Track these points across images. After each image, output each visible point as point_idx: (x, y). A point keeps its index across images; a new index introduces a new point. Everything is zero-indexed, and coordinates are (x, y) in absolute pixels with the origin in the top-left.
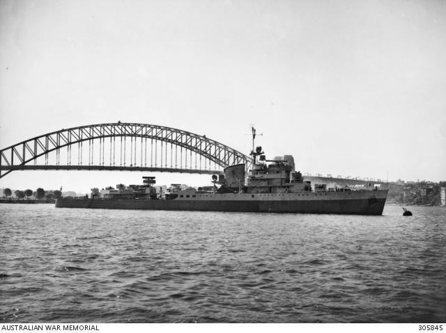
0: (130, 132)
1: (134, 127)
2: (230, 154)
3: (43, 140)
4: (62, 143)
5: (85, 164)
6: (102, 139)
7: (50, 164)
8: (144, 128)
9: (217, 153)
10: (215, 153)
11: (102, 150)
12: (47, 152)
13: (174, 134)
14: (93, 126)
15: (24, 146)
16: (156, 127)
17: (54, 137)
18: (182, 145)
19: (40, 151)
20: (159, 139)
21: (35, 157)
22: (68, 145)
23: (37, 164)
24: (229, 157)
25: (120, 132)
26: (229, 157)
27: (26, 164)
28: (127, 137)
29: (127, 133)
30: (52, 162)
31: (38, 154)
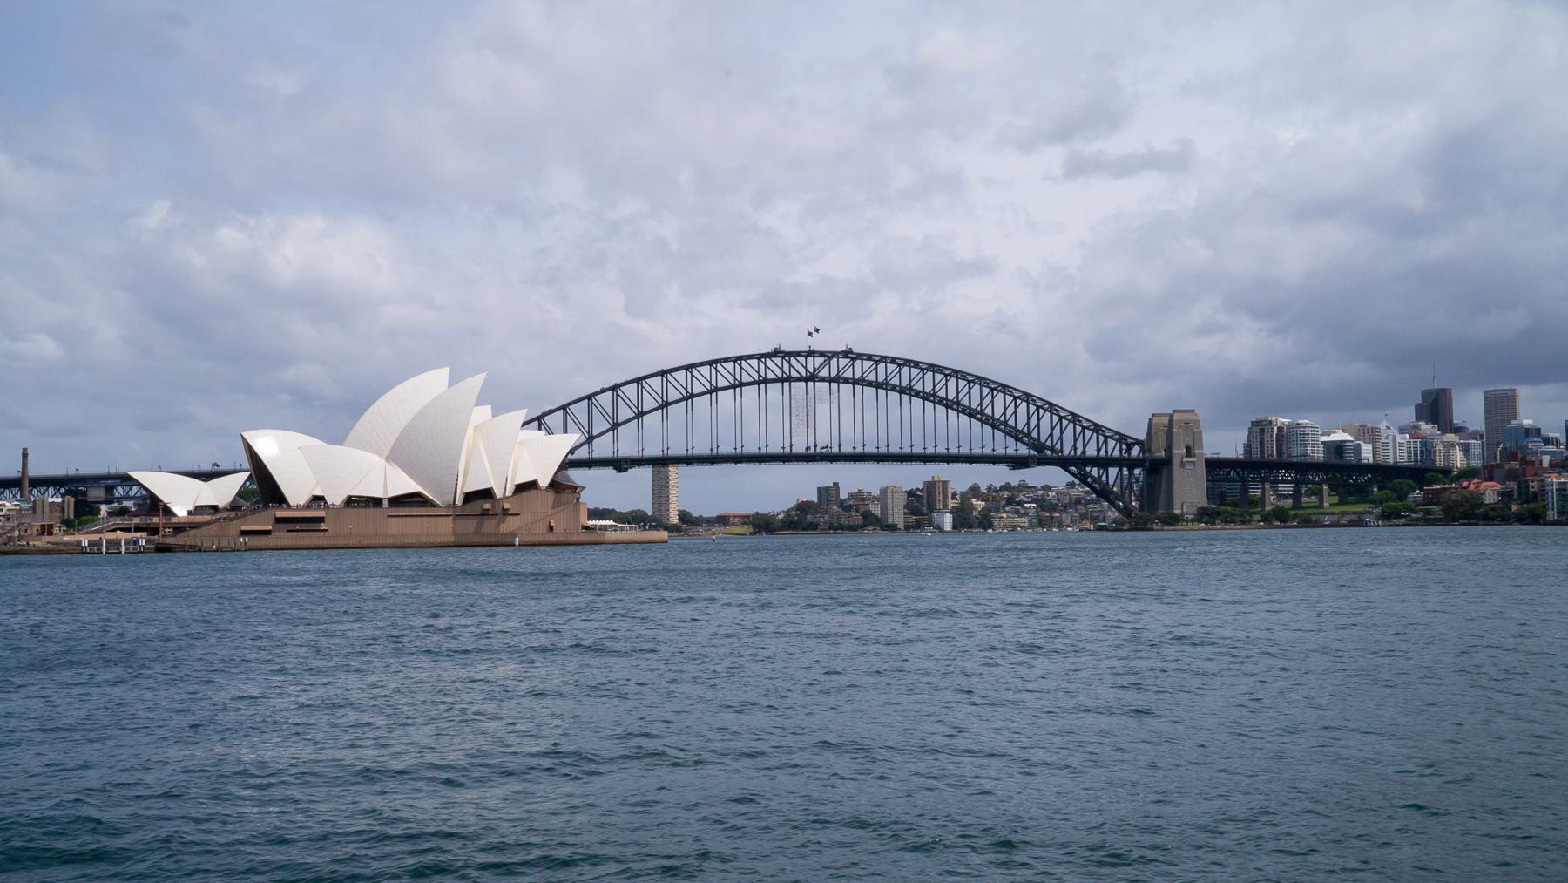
0: (803, 373)
1: (810, 359)
4: (649, 403)
5: (702, 449)
8: (835, 360)
9: (1033, 421)
10: (1028, 424)
12: (615, 426)
14: (741, 358)
15: (565, 414)
20: (894, 388)
22: (661, 407)
23: (597, 455)
25: (779, 374)
29: (794, 374)
30: (627, 450)
31: (595, 433)
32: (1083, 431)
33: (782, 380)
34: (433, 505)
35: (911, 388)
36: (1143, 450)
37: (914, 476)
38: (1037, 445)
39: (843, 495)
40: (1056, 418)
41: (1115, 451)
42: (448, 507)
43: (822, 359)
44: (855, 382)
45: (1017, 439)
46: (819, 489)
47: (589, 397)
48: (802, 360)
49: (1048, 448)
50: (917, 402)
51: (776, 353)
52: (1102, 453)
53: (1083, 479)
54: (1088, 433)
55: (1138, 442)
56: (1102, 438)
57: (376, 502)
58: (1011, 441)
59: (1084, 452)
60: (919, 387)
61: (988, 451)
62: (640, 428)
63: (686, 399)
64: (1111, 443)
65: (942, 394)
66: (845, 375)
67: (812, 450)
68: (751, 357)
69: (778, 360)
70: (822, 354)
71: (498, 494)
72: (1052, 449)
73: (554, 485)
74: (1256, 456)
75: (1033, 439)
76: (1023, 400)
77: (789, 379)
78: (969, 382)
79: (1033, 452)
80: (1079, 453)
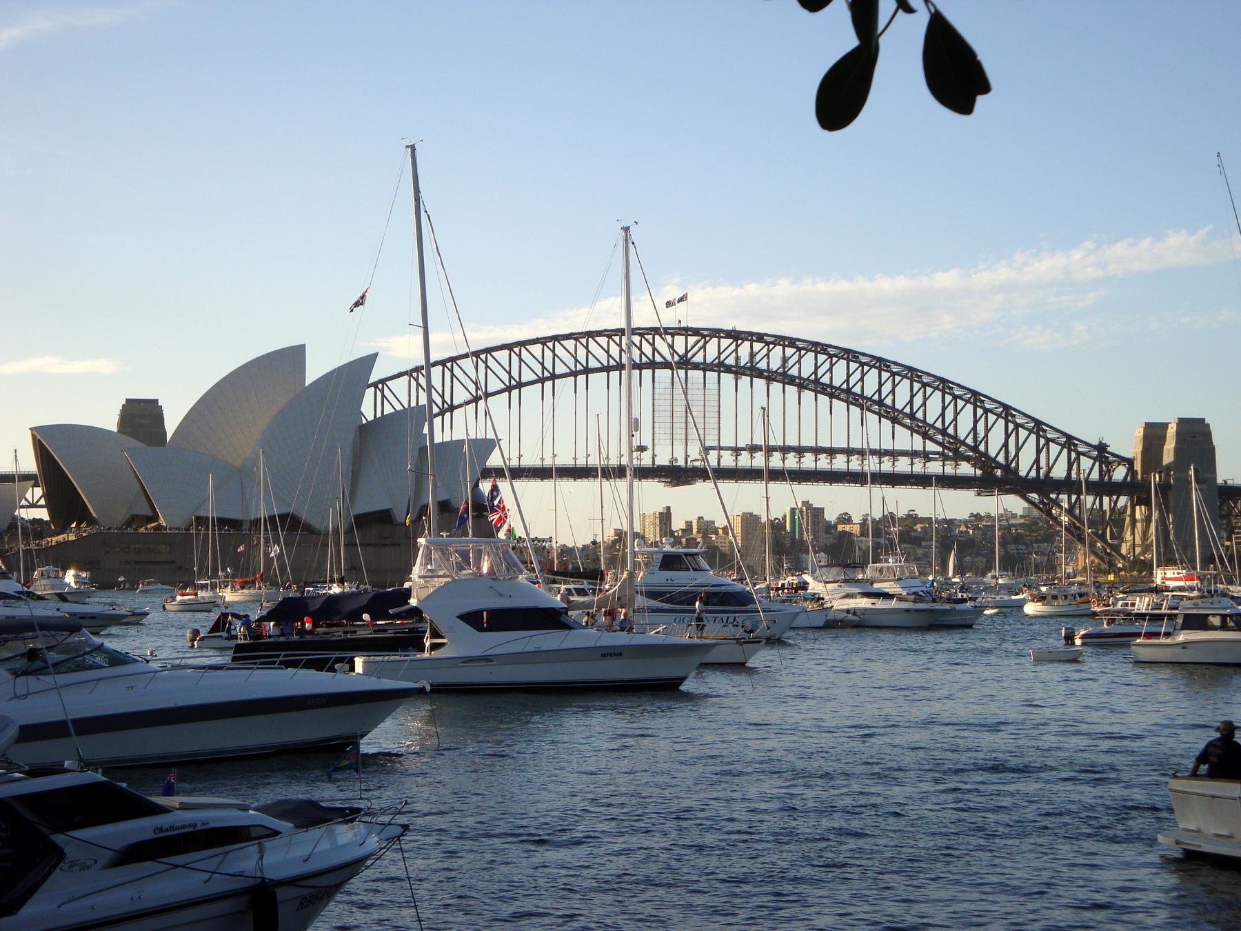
2: (1023, 433)
4: (461, 396)
6: (548, 384)
13: (809, 359)
16: (716, 333)
18: (831, 392)
29: (658, 359)
32: (1047, 444)
35: (817, 381)
36: (1131, 469)
38: (982, 460)
41: (1088, 468)
49: (999, 466)
55: (1122, 460)
67: (681, 462)
68: (600, 333)
70: (696, 332)
72: (1006, 468)
75: (980, 453)
76: (967, 401)
78: (893, 374)
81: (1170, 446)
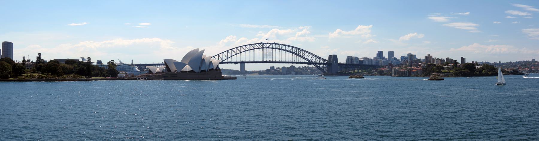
0: (266, 47)
1: (268, 44)
3: (230, 51)
4: (238, 52)
7: (233, 61)
10: (307, 57)
11: (254, 54)
12: (232, 56)
17: (235, 50)
19: (229, 56)
20: (283, 50)
21: (227, 58)
23: (228, 61)
24: (313, 58)
26: (313, 58)
27: (224, 62)
28: (278, 50)
29: (264, 47)
30: (234, 61)
31: (228, 57)
32: (317, 58)
33: (262, 48)
34: (195, 72)
36: (327, 61)
37: (288, 65)
38: (308, 60)
39: (275, 68)
40: (312, 56)
42: (198, 73)
43: (270, 44)
44: (275, 49)
45: (305, 59)
46: (271, 67)
47: (227, 51)
48: (266, 44)
50: (287, 52)
51: (261, 43)
52: (320, 62)
53: (317, 66)
54: (318, 58)
55: (327, 60)
56: (320, 59)
57: (186, 72)
58: (304, 60)
59: (317, 62)
60: (287, 50)
61: (300, 61)
62: (236, 57)
63: (245, 51)
64: (322, 60)
65: (291, 51)
66: (274, 47)
69: (262, 44)
70: (270, 43)
71: (206, 70)
72: (311, 61)
73: (216, 69)
74: (348, 63)
77: (264, 48)
79: (308, 62)
80: (316, 62)
81: (332, 58)
